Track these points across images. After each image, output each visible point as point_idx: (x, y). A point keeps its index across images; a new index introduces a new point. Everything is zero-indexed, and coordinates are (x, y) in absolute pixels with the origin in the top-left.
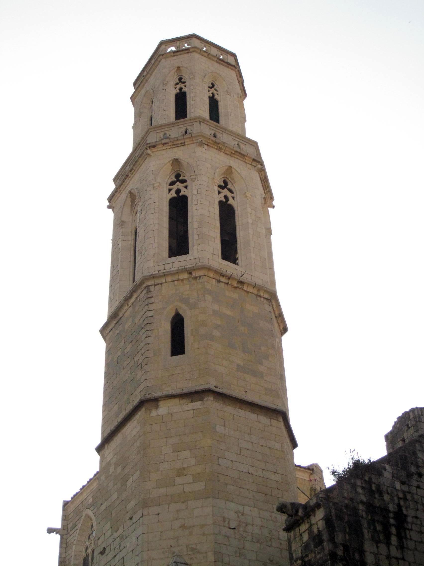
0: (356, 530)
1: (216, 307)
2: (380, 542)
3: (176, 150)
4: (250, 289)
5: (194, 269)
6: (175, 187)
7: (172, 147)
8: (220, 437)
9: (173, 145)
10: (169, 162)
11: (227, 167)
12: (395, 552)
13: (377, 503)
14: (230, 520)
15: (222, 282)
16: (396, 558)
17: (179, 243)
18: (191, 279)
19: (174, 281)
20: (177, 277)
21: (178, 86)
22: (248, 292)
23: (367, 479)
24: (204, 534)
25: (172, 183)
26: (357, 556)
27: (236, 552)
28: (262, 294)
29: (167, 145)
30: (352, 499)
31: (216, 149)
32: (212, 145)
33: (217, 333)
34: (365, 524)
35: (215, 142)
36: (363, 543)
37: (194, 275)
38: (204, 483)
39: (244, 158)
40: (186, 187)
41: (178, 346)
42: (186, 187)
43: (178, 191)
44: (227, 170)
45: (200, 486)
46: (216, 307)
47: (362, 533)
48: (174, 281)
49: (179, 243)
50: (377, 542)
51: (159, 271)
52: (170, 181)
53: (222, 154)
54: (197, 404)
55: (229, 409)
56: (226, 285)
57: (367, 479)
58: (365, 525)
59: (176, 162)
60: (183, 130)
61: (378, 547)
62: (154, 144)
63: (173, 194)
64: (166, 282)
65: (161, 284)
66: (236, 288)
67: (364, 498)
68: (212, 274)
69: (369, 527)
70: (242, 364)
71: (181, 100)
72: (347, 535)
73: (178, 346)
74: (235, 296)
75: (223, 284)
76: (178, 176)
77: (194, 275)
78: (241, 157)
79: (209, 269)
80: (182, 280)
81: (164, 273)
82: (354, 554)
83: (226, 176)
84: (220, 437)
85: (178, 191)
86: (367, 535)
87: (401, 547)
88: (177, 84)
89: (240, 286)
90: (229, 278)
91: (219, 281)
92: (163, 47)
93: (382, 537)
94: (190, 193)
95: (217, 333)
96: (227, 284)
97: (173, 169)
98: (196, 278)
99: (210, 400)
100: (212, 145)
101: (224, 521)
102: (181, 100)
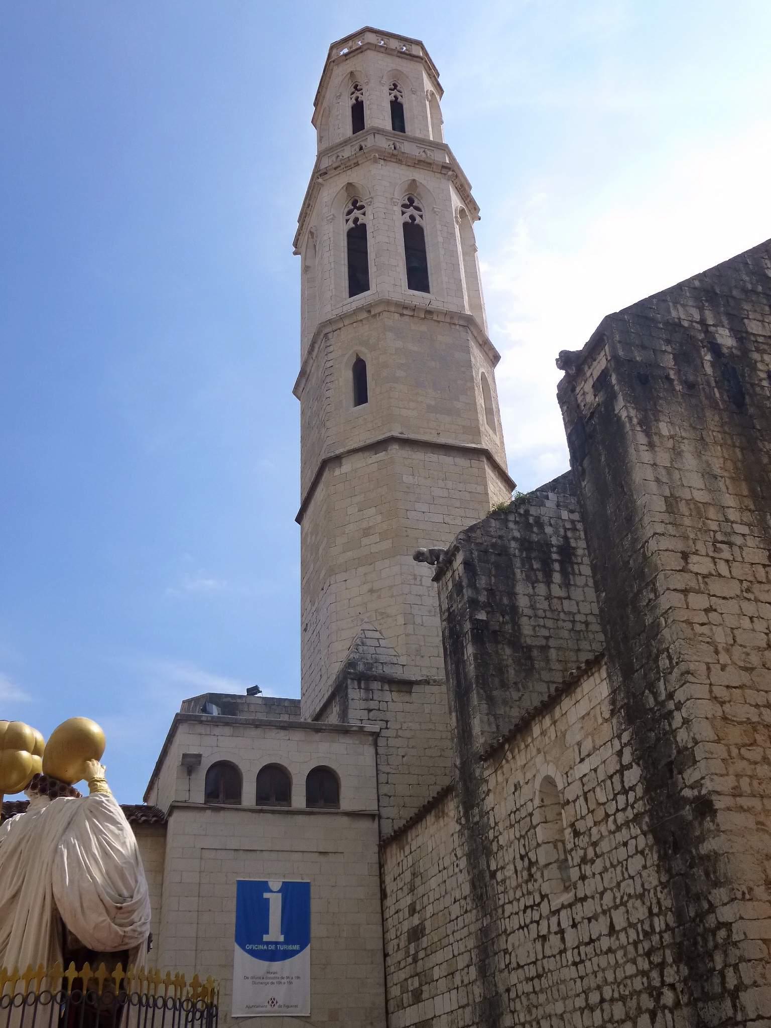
0: (505, 572)
1: (399, 344)
2: (537, 581)
3: (349, 172)
5: (371, 305)
6: (352, 217)
8: (408, 488)
12: (556, 591)
13: (535, 538)
14: (422, 576)
16: (560, 598)
17: (358, 280)
20: (355, 318)
21: (354, 96)
23: (522, 511)
24: (392, 596)
25: (349, 213)
26: (505, 601)
27: (430, 611)
30: (500, 537)
33: (400, 373)
34: (517, 563)
36: (514, 586)
37: (373, 313)
38: (390, 541)
40: (364, 214)
41: (361, 397)
42: (364, 214)
43: (356, 220)
45: (387, 545)
46: (399, 344)
47: (514, 574)
49: (358, 280)
50: (534, 583)
52: (347, 210)
54: (381, 455)
55: (419, 456)
57: (522, 511)
58: (518, 564)
59: (350, 186)
60: (357, 147)
61: (534, 588)
63: (351, 224)
67: (517, 534)
69: (523, 565)
70: (433, 403)
71: (358, 111)
72: (493, 578)
73: (361, 397)
76: (355, 203)
77: (373, 313)
79: (388, 302)
80: (361, 320)
82: (501, 599)
84: (408, 488)
85: (356, 220)
86: (519, 574)
87: (566, 584)
88: (353, 93)
91: (402, 315)
92: (334, 51)
93: (540, 575)
94: (367, 220)
95: (400, 373)
97: (348, 195)
98: (375, 316)
99: (394, 448)
101: (415, 579)
102: (358, 111)
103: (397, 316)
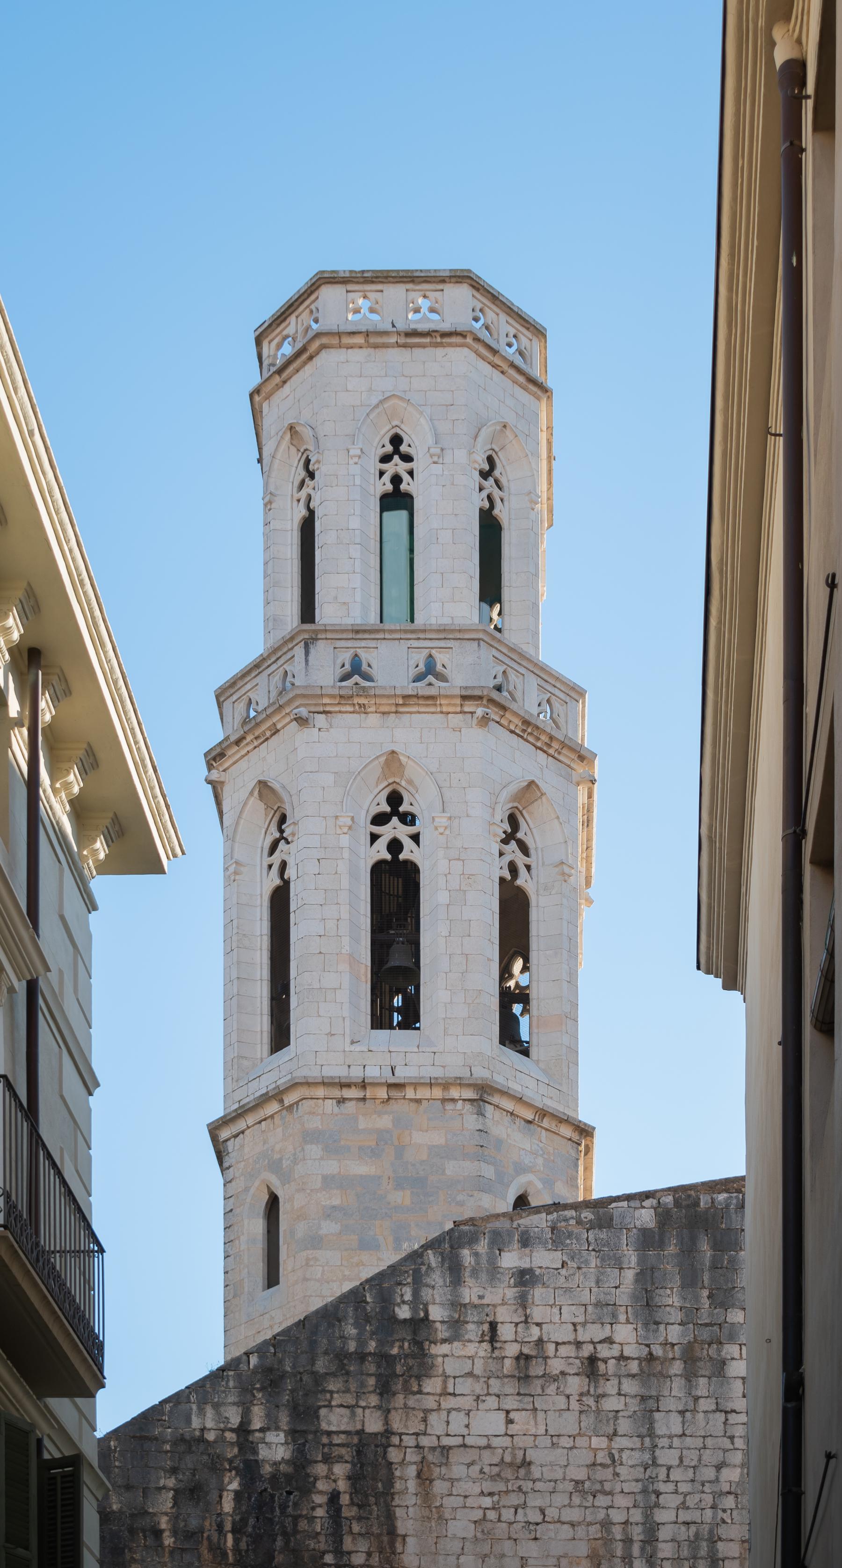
4: (423, 1093)
7: (256, 743)
9: (256, 738)
10: (251, 793)
11: (383, 759)
15: (351, 1099)
18: (284, 1112)
19: (260, 1122)
22: (418, 1101)
28: (455, 1093)
29: (245, 742)
31: (353, 712)
32: (337, 709)
35: (341, 697)
37: (287, 1103)
39: (435, 705)
44: (388, 763)
48: (260, 1122)
51: (239, 1102)
53: (373, 719)
56: (361, 1104)
62: (218, 750)
64: (248, 1127)
65: (243, 1132)
66: (389, 1099)
68: (320, 1092)
74: (385, 1122)
75: (353, 1103)
77: (287, 1103)
78: (427, 705)
80: (272, 1117)
81: (236, 1110)
83: (391, 781)
89: (394, 1093)
90: (363, 1085)
91: (341, 1101)
96: (364, 1099)
97: (268, 807)
98: (291, 1106)
100: (337, 709)
103: (330, 1105)
